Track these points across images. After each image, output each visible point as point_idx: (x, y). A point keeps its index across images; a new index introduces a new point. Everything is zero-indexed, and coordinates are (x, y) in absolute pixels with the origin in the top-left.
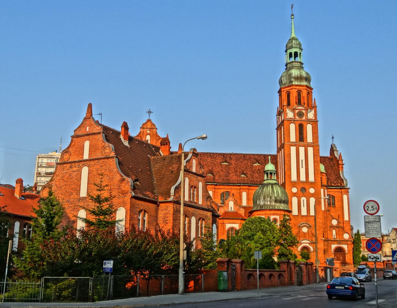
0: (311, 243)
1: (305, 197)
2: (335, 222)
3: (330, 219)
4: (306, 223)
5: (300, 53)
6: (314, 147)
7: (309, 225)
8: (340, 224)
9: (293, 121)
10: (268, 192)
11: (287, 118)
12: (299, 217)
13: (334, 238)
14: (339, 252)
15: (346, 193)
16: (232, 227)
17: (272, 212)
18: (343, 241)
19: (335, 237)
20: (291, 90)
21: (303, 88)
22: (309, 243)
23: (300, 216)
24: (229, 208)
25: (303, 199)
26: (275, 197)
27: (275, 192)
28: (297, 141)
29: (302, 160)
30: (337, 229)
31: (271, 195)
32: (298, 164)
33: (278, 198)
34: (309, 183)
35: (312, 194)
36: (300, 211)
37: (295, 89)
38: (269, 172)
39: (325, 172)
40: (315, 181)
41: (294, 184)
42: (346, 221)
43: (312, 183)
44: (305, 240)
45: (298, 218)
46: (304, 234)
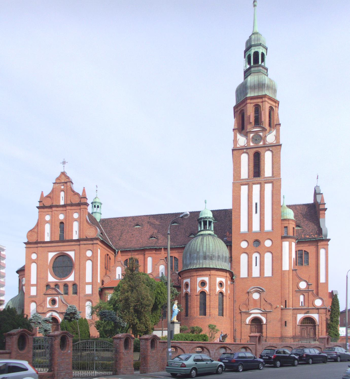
0: (265, 313)
1: (258, 252)
2: (303, 285)
3: (297, 281)
4: (257, 288)
8: (310, 287)
10: (196, 246)
13: (301, 305)
14: (308, 323)
15: (325, 246)
18: (313, 309)
19: (303, 305)
22: (260, 314)
25: (256, 255)
26: (203, 252)
27: (205, 245)
28: (250, 177)
29: (256, 204)
30: (306, 295)
31: (198, 250)
32: (250, 209)
36: (250, 271)
38: (203, 220)
39: (293, 218)
40: (273, 230)
41: (244, 237)
42: (323, 283)
43: (268, 233)
44: (256, 309)
45: (247, 281)
46: (255, 301)
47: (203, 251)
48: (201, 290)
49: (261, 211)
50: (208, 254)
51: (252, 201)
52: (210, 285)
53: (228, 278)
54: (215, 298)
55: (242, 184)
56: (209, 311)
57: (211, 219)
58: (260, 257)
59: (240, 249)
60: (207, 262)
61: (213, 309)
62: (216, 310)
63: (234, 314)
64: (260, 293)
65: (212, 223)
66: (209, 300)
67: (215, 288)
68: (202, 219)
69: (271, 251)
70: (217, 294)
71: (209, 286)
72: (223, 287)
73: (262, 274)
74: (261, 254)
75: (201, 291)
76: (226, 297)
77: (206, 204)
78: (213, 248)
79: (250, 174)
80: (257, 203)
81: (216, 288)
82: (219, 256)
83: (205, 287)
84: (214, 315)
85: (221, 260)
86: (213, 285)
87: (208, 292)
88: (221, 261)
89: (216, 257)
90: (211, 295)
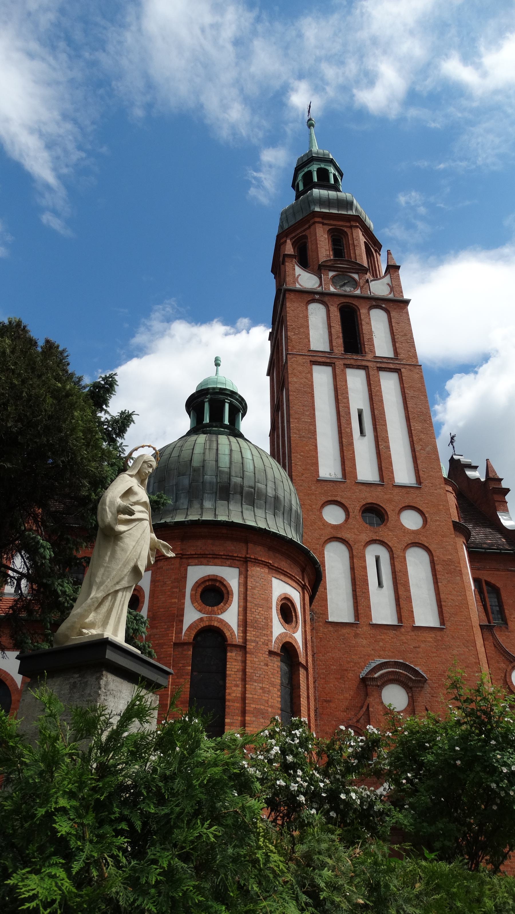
5: (334, 175)
6: (403, 370)
7: (416, 673)
9: (317, 297)
11: (298, 286)
12: (359, 631)
17: (199, 543)
20: (308, 231)
21: (348, 224)
23: (364, 629)
31: (196, 463)
32: (343, 421)
34: (397, 490)
35: (414, 532)
36: (361, 600)
37: (323, 224)
45: (356, 635)
47: (217, 467)
48: (201, 619)
49: (378, 430)
50: (236, 480)
54: (267, 665)
57: (237, 400)
58: (392, 558)
59: (322, 527)
60: (231, 507)
64: (410, 684)
66: (240, 675)
68: (207, 394)
69: (427, 545)
70: (276, 650)
72: (294, 624)
73: (404, 614)
74: (394, 549)
75: (202, 625)
77: (219, 368)
78: (256, 465)
79: (334, 344)
80: (362, 410)
82: (276, 498)
83: (223, 611)
85: (286, 515)
88: (286, 521)
90: (250, 646)
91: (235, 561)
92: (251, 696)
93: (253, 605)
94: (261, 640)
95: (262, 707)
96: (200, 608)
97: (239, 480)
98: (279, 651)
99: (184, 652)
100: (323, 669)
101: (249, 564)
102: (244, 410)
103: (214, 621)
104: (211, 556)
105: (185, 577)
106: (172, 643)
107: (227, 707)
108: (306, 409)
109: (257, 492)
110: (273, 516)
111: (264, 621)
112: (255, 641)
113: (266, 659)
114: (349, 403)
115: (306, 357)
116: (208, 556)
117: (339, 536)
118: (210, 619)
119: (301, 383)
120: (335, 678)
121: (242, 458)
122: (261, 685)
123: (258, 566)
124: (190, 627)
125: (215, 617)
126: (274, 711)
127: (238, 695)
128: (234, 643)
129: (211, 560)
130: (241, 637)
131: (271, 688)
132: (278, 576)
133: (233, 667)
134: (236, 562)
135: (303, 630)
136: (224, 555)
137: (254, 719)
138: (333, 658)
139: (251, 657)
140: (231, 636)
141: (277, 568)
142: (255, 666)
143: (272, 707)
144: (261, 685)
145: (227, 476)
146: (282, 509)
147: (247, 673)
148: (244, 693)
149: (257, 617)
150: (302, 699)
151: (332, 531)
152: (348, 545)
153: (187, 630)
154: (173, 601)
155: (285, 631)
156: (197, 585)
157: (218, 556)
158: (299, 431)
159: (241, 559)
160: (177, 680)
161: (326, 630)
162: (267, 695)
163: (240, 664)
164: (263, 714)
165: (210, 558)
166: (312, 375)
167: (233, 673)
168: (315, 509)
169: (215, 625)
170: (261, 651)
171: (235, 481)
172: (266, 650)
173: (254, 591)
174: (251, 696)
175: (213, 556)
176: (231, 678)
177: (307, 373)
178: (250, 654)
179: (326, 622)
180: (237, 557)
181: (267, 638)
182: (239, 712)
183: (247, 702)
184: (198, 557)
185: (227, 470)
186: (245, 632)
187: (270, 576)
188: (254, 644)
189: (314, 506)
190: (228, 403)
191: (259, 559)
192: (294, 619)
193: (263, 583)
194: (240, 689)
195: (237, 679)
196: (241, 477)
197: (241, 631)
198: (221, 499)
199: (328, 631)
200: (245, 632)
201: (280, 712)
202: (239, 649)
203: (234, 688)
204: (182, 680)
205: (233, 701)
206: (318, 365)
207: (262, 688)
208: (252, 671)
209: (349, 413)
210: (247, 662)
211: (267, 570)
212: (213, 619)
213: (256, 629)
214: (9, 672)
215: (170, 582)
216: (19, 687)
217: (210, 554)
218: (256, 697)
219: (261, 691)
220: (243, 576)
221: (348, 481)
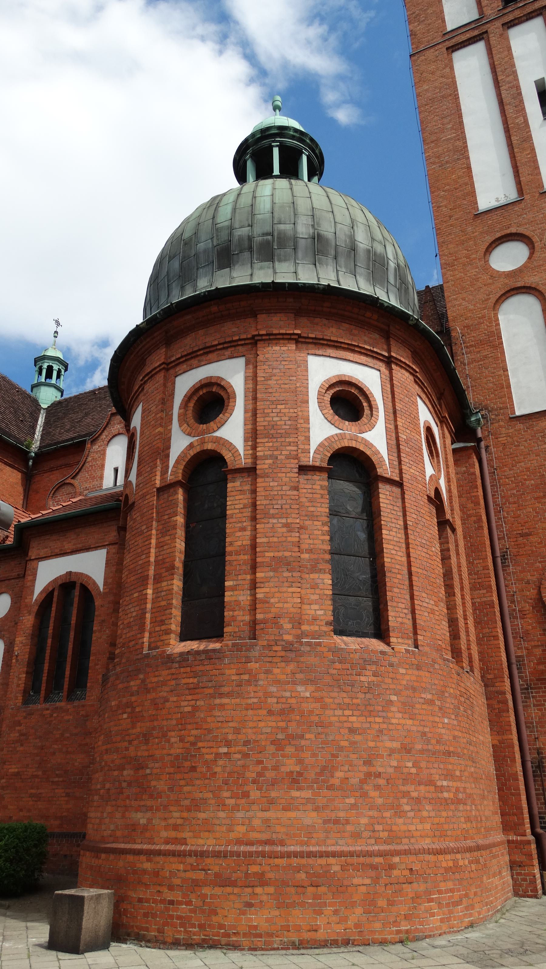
16: (70, 573)
24: (101, 477)
32: (510, 110)
33: (242, 232)
47: (214, 224)
48: (191, 446)
51: (516, 79)
52: (255, 399)
53: (401, 375)
54: (296, 488)
55: (452, 46)
56: (244, 597)
57: (293, 138)
61: (286, 574)
62: (314, 587)
63: (512, 648)
65: (305, 159)
66: (248, 512)
67: (295, 419)
68: (248, 147)
70: (317, 464)
71: (246, 411)
72: (364, 419)
75: (192, 453)
76: (397, 490)
81: (307, 420)
84: (287, 626)
85: (342, 260)
86: (277, 402)
87: (241, 452)
89: (302, 244)
90: (262, 466)
91: (237, 348)
92: (265, 540)
93: (268, 403)
94: (284, 453)
95: (287, 554)
96: (188, 431)
97: (245, 231)
98: (325, 465)
99: (170, 498)
100: (513, 489)
101: (259, 344)
102: (313, 151)
103: (208, 442)
104: (202, 352)
105: (172, 395)
106: (155, 490)
107: (227, 563)
108: (446, 121)
109: (278, 238)
110: (312, 266)
111: (289, 423)
112: (271, 456)
113: (293, 479)
114: (518, 80)
115: (440, 46)
116: (199, 353)
117: (519, 284)
118: (203, 442)
119: (436, 88)
120: (536, 499)
121: (254, 197)
122: (284, 521)
123: (276, 344)
124: (177, 462)
125: (209, 437)
126: (313, 556)
127: (245, 543)
128: (237, 467)
129: (203, 358)
130: (250, 456)
131: (307, 523)
132: (320, 352)
133: (236, 502)
134: (241, 348)
135: (392, 427)
136: (219, 344)
137: (272, 574)
138: (528, 469)
139: (265, 482)
140: (233, 458)
141: (315, 338)
142: (272, 493)
143: (310, 551)
144: (284, 521)
145: (227, 232)
146: (333, 252)
147: (258, 507)
148: (254, 538)
149: (275, 419)
150: (384, 532)
151: (507, 281)
152: (537, 294)
153: (174, 467)
154: (157, 431)
155: (339, 431)
156: (188, 398)
157: (211, 349)
158: (438, 157)
159: (247, 342)
160: (162, 540)
161: (511, 431)
162: (297, 534)
163: (248, 495)
164: (288, 564)
165: (201, 355)
166: (452, 68)
167: (238, 511)
168: (475, 259)
169: (209, 448)
170: (283, 470)
171: (239, 233)
172: (293, 466)
173: (269, 382)
174: (265, 540)
175: (205, 351)
176: (234, 520)
177: (444, 68)
178: (262, 477)
179: (511, 418)
180: (240, 340)
181: (295, 448)
182: (247, 568)
183: (258, 550)
184: (186, 360)
185: (227, 224)
186: (254, 448)
187: (302, 355)
188: (270, 461)
189: (474, 256)
190: (277, 146)
191: (274, 332)
192: (367, 411)
193: (286, 367)
194: (248, 533)
195: (244, 519)
196: (249, 226)
197: (249, 448)
198: (221, 267)
199: (515, 430)
200: (254, 448)
201: (328, 557)
202: (246, 474)
203: (239, 534)
204: (167, 538)
205: (238, 553)
206: (461, 48)
207: (286, 525)
208: (265, 502)
209: (520, 94)
210: (258, 490)
211: (293, 347)
212: (206, 440)
213: (273, 437)
214: (90, 575)
215: (154, 407)
216: (102, 590)
217: (200, 350)
218: (275, 540)
219: (285, 530)
220: (251, 366)
221: (526, 197)
